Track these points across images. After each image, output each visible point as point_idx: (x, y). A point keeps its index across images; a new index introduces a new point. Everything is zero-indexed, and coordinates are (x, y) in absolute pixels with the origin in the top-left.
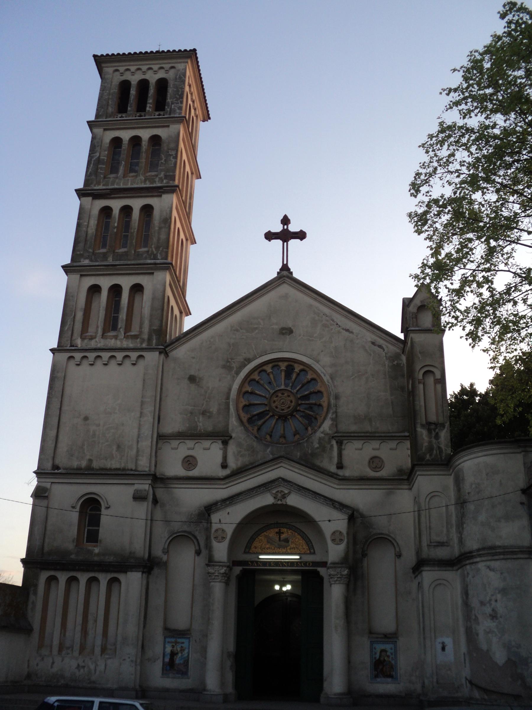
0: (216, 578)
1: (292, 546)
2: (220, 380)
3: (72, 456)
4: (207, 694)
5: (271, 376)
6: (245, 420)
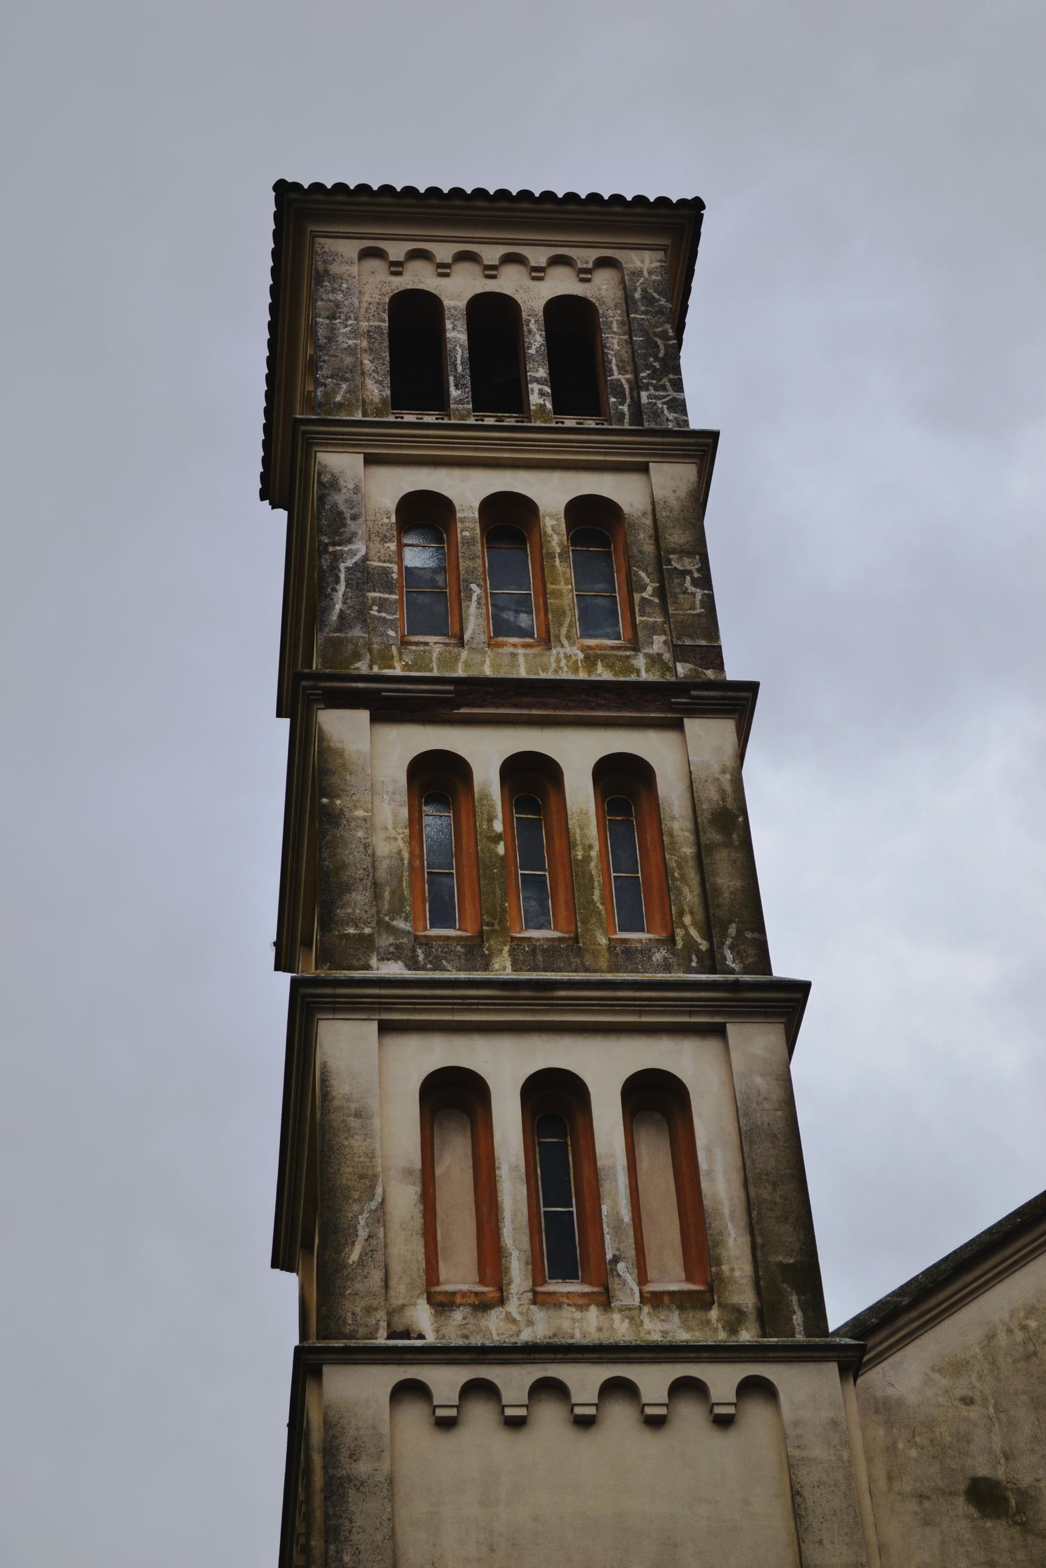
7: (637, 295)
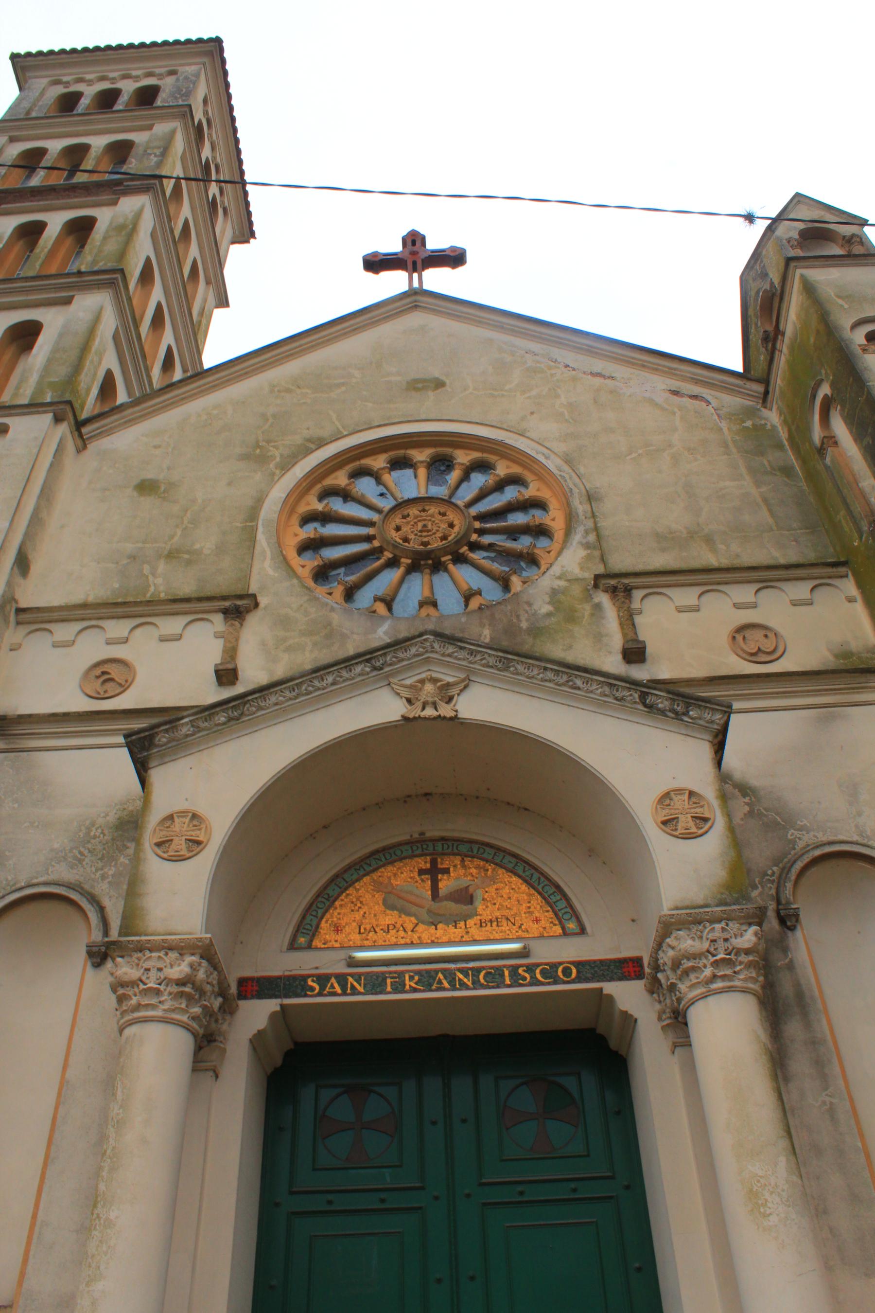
2: (230, 484)
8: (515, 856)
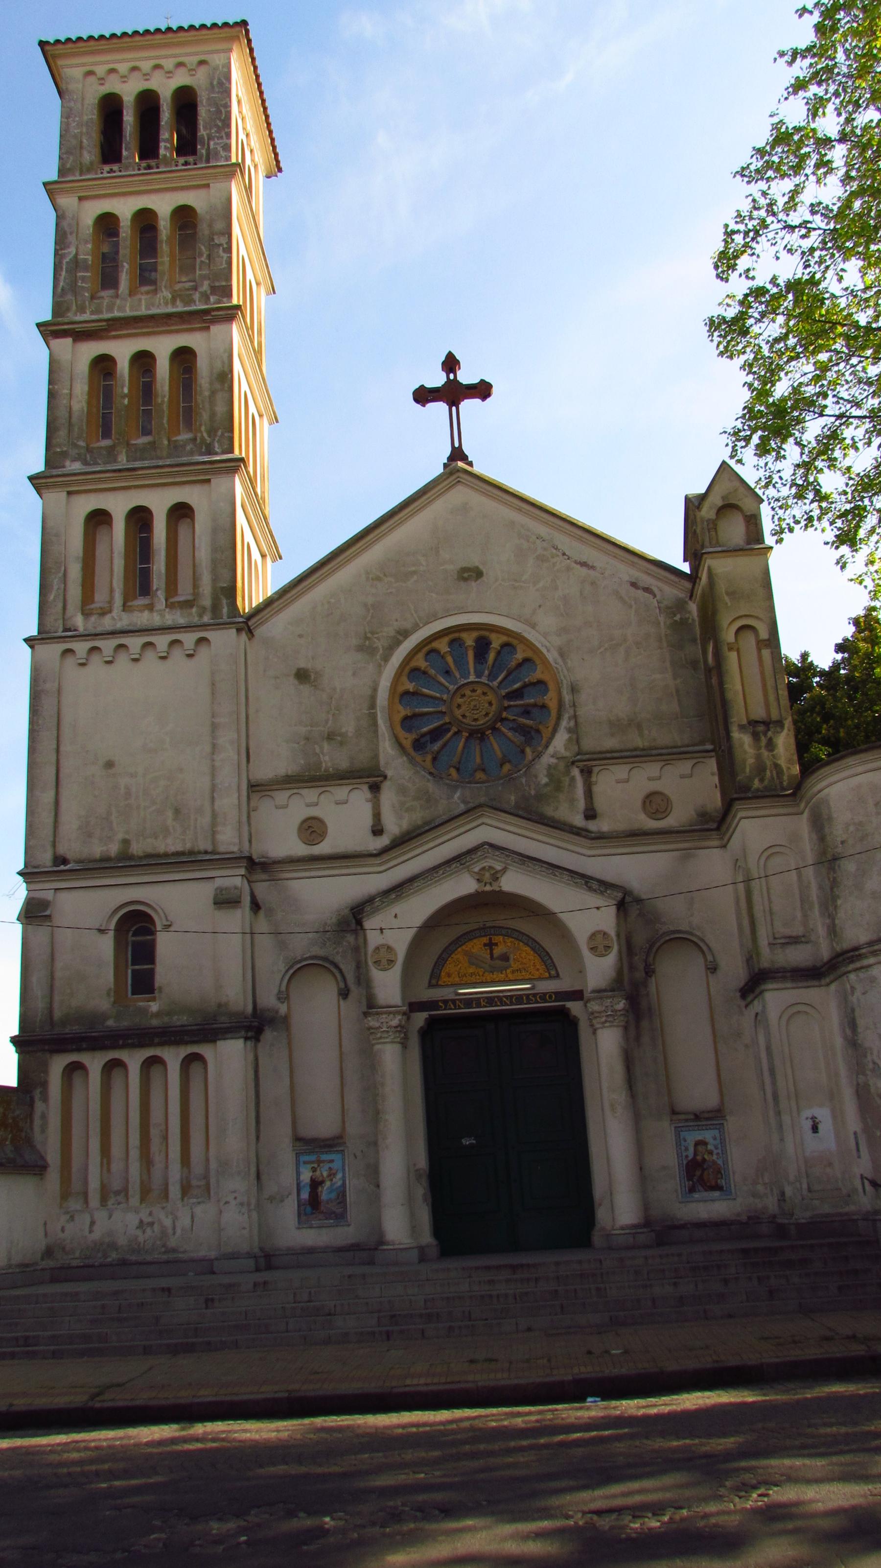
0: (385, 1035)
1: (515, 966)
2: (354, 674)
3: (90, 835)
4: (387, 1250)
5: (449, 659)
6: (408, 744)
7: (215, 83)
8: (528, 936)
